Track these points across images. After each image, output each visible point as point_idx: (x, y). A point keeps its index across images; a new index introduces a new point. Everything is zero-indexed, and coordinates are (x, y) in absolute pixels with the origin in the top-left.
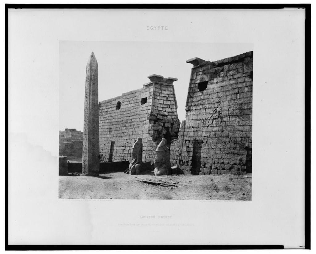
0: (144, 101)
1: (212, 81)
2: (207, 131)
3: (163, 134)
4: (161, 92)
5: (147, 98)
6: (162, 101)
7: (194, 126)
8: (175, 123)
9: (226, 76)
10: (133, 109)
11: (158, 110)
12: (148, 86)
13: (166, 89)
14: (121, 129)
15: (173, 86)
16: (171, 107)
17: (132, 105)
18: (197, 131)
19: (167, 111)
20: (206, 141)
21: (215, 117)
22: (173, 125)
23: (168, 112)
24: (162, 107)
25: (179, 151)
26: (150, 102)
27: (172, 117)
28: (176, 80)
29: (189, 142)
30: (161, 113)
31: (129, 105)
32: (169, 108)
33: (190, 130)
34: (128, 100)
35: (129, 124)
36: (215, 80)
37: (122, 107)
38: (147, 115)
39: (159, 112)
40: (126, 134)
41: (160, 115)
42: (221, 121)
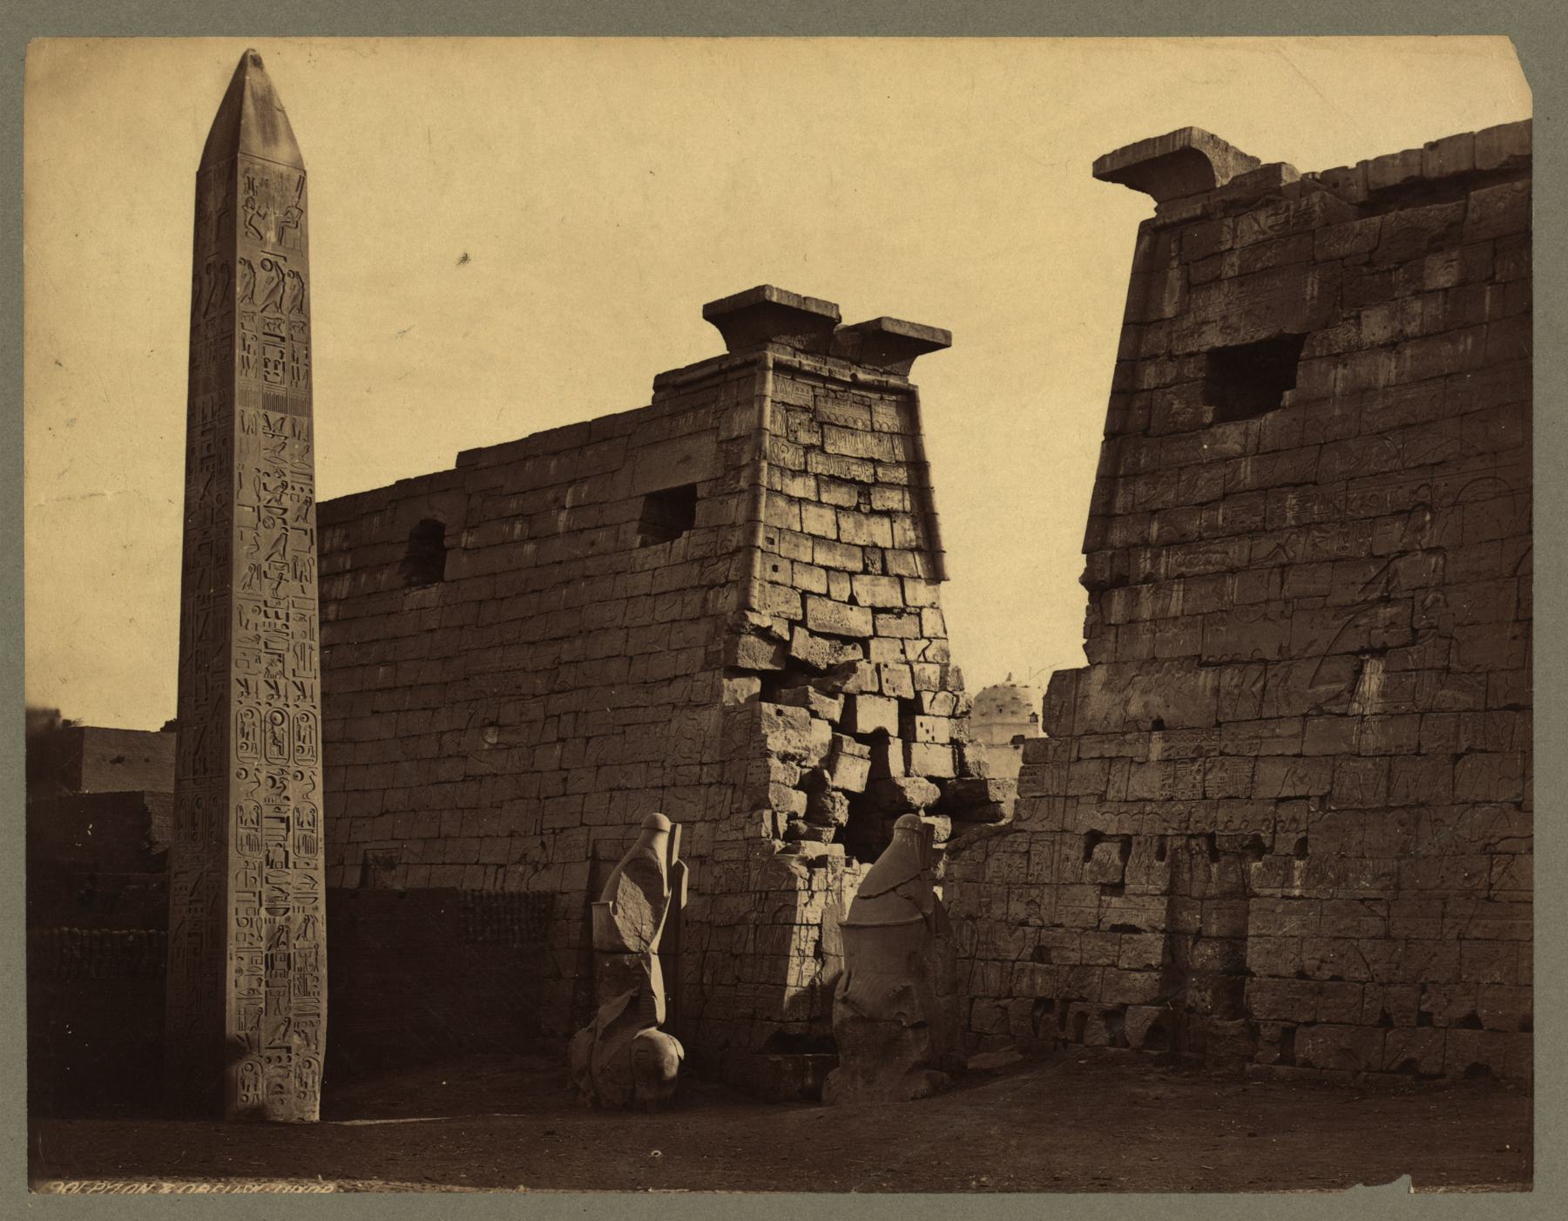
1: (1342, 336)
2: (1299, 755)
3: (846, 792)
4: (815, 440)
5: (701, 492)
6: (829, 515)
7: (1168, 715)
8: (927, 697)
9: (1491, 280)
10: (568, 582)
11: (793, 588)
13: (859, 417)
15: (908, 401)
18: (1200, 753)
19: (864, 599)
20: (1294, 837)
21: (1379, 637)
22: (919, 719)
23: (876, 611)
24: (827, 569)
25: (1024, 923)
26: (733, 526)
27: (903, 652)
28: (940, 339)
29: (1125, 854)
30: (821, 613)
31: (529, 548)
33: (1127, 751)
35: (535, 710)
36: (1375, 326)
37: (456, 565)
39: (804, 606)
41: (812, 634)
42: (1447, 670)
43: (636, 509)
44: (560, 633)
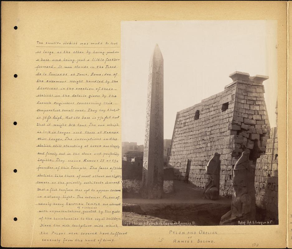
0: (225, 106)
4: (246, 94)
12: (229, 88)
14: (198, 144)
15: (262, 86)
16: (260, 113)
17: (212, 113)
19: (254, 118)
23: (256, 120)
27: (261, 127)
32: (258, 114)
34: (207, 107)
37: (200, 116)
38: (228, 124)
40: (204, 149)
43: (221, 106)
44: (211, 126)
